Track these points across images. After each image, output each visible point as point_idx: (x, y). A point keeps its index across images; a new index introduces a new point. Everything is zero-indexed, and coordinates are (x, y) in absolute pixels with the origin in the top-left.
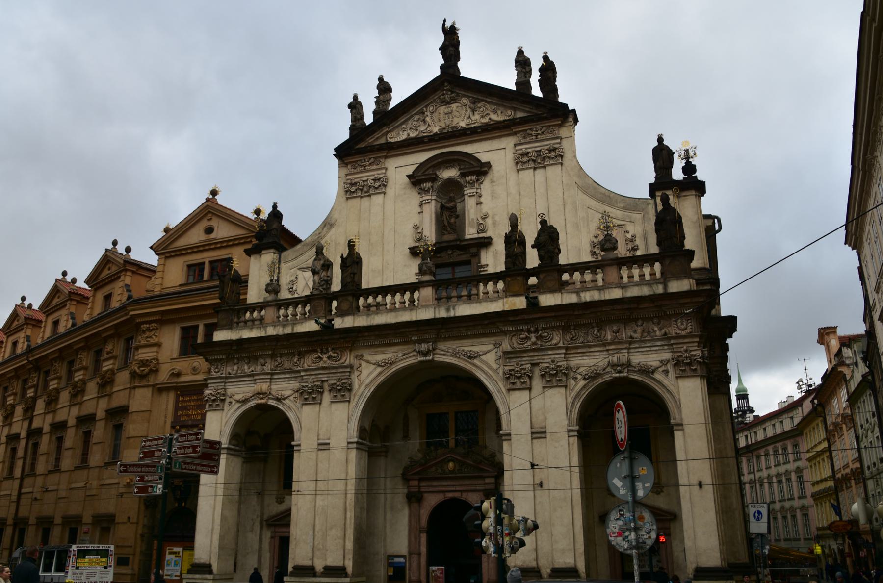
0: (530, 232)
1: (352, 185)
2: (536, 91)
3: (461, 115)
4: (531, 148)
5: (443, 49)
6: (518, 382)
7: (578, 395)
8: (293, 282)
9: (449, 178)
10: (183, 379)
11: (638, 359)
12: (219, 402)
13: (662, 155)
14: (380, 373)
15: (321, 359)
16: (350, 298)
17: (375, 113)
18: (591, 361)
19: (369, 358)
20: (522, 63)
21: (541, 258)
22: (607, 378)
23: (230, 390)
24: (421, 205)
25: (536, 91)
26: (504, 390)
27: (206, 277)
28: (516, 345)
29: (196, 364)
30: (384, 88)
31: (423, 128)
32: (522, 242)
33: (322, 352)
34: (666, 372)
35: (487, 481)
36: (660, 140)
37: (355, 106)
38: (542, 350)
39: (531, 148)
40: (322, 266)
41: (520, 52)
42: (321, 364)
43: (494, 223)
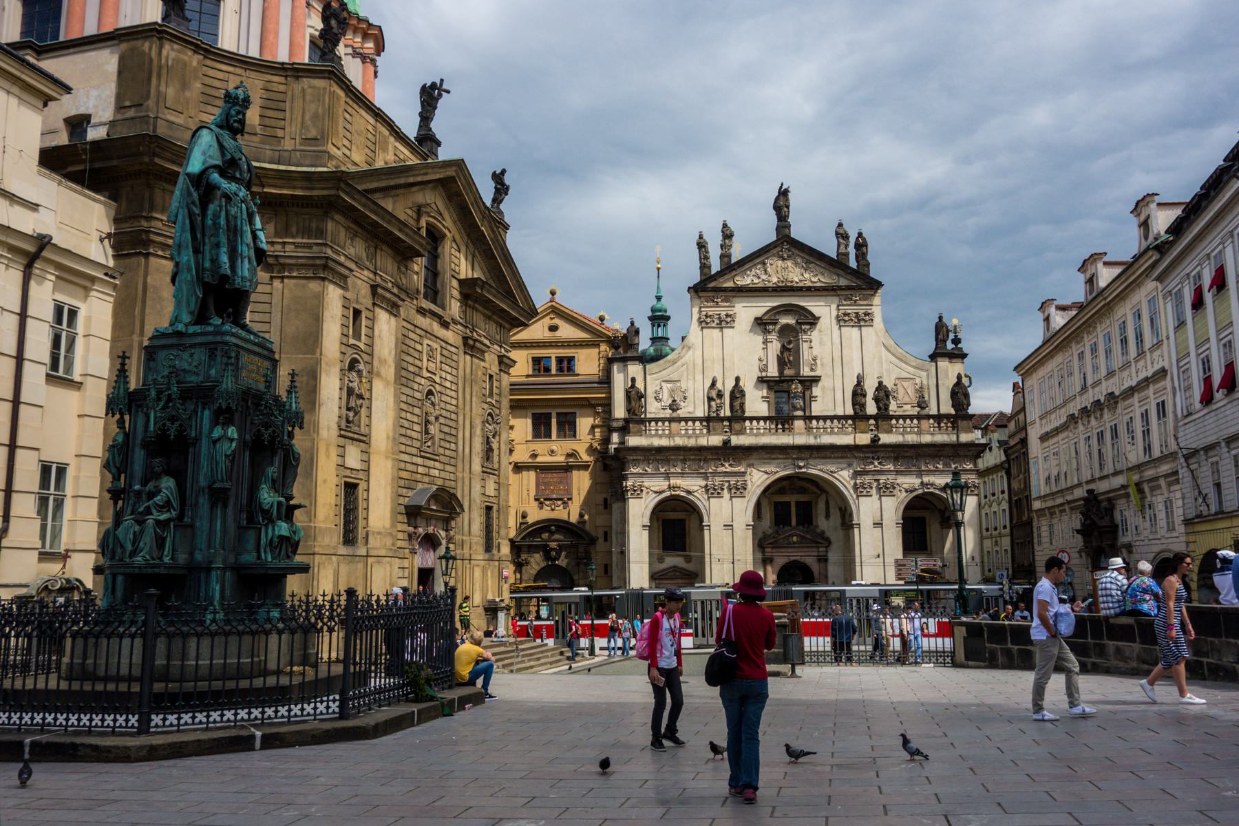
0: (870, 387)
1: (707, 316)
2: (853, 263)
3: (796, 274)
4: (851, 310)
5: (777, 208)
9: (788, 325)
10: (539, 459)
12: (638, 492)
13: (941, 329)
17: (722, 256)
20: (842, 235)
21: (879, 408)
22: (921, 491)
23: (646, 484)
24: (765, 342)
25: (853, 263)
27: (554, 371)
29: (554, 448)
30: (727, 235)
31: (764, 277)
32: (865, 396)
36: (940, 318)
37: (702, 245)
39: (851, 310)
40: (714, 395)
41: (840, 225)
42: (723, 469)
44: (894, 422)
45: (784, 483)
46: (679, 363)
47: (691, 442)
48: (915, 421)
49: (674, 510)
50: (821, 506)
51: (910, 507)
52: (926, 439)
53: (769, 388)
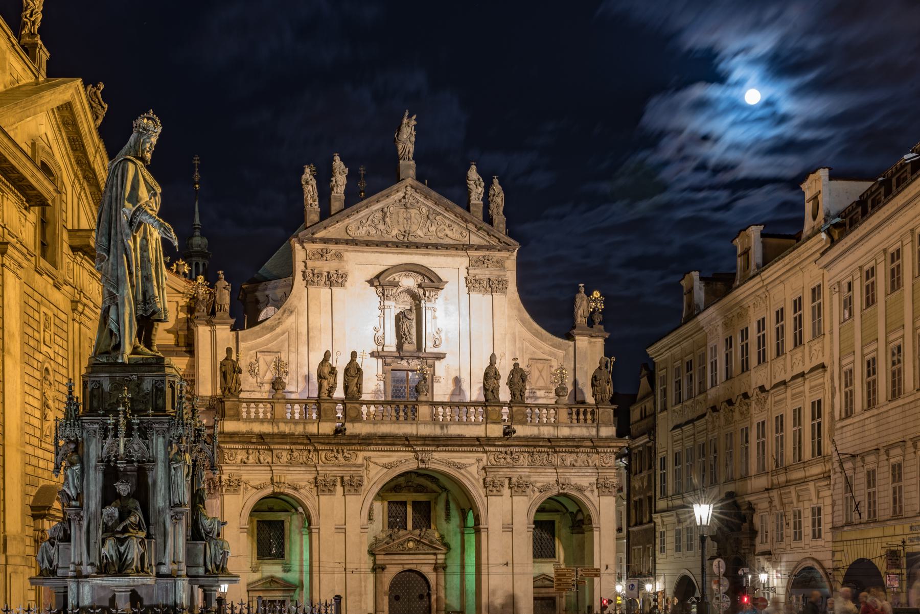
6: (494, 490)
7: (536, 504)
8: (251, 364)
11: (575, 480)
14: (386, 473)
15: (336, 458)
16: (357, 405)
18: (545, 479)
19: (377, 461)
21: (513, 394)
22: (555, 492)
24: (382, 308)
26: (483, 496)
28: (495, 463)
33: (338, 452)
34: (592, 491)
35: (439, 557)
38: (513, 467)
43: (447, 339)
44: (528, 410)
45: (402, 479)
46: (278, 330)
47: (299, 429)
48: (552, 411)
49: (271, 510)
50: (441, 507)
51: (541, 510)
52: (565, 432)
53: (385, 364)
